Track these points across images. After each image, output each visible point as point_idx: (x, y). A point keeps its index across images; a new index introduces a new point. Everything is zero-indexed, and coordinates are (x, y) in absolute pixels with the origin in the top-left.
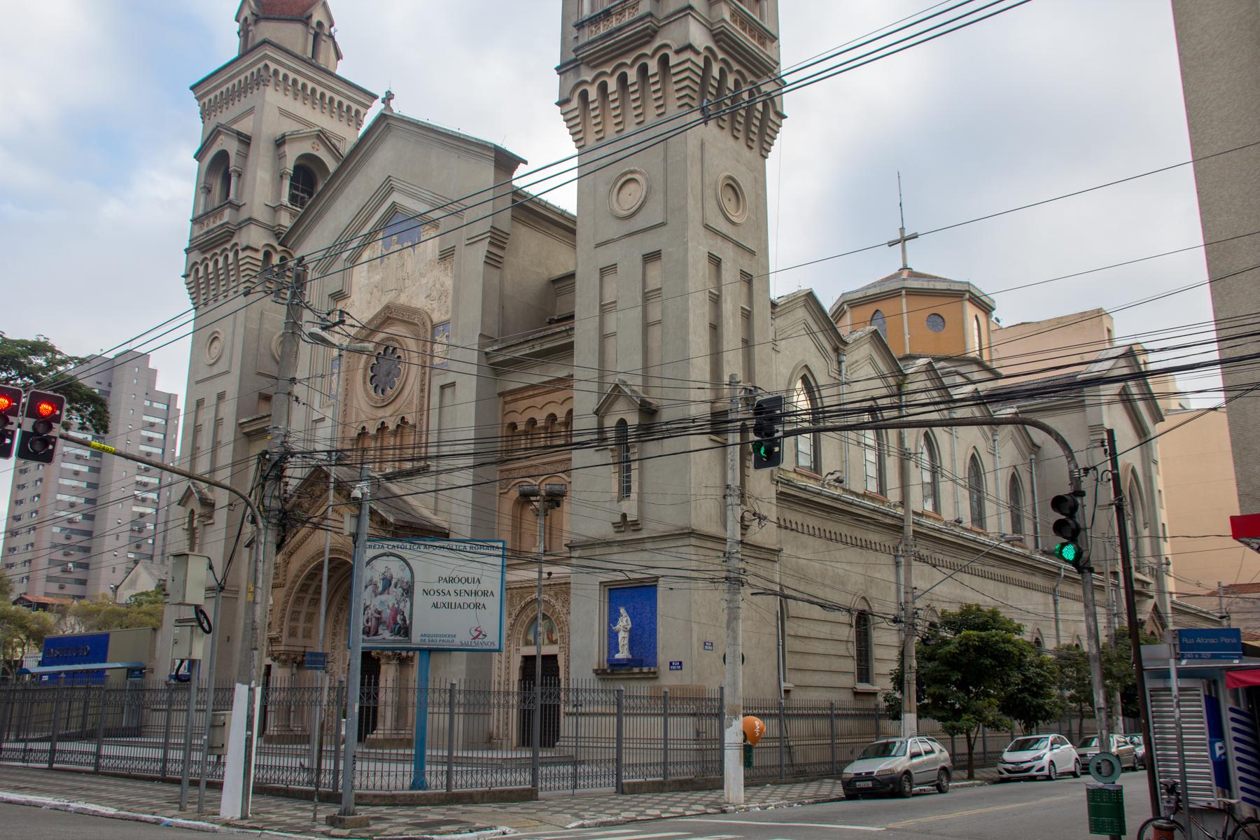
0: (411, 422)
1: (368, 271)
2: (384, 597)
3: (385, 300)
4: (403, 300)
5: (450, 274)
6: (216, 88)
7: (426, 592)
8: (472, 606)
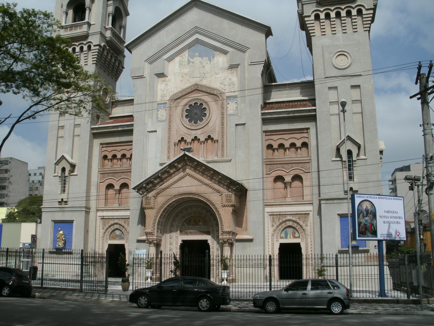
0: (215, 139)
1: (180, 67)
2: (367, 218)
3: (193, 81)
4: (205, 82)
5: (236, 76)
7: (381, 217)
8: (396, 223)
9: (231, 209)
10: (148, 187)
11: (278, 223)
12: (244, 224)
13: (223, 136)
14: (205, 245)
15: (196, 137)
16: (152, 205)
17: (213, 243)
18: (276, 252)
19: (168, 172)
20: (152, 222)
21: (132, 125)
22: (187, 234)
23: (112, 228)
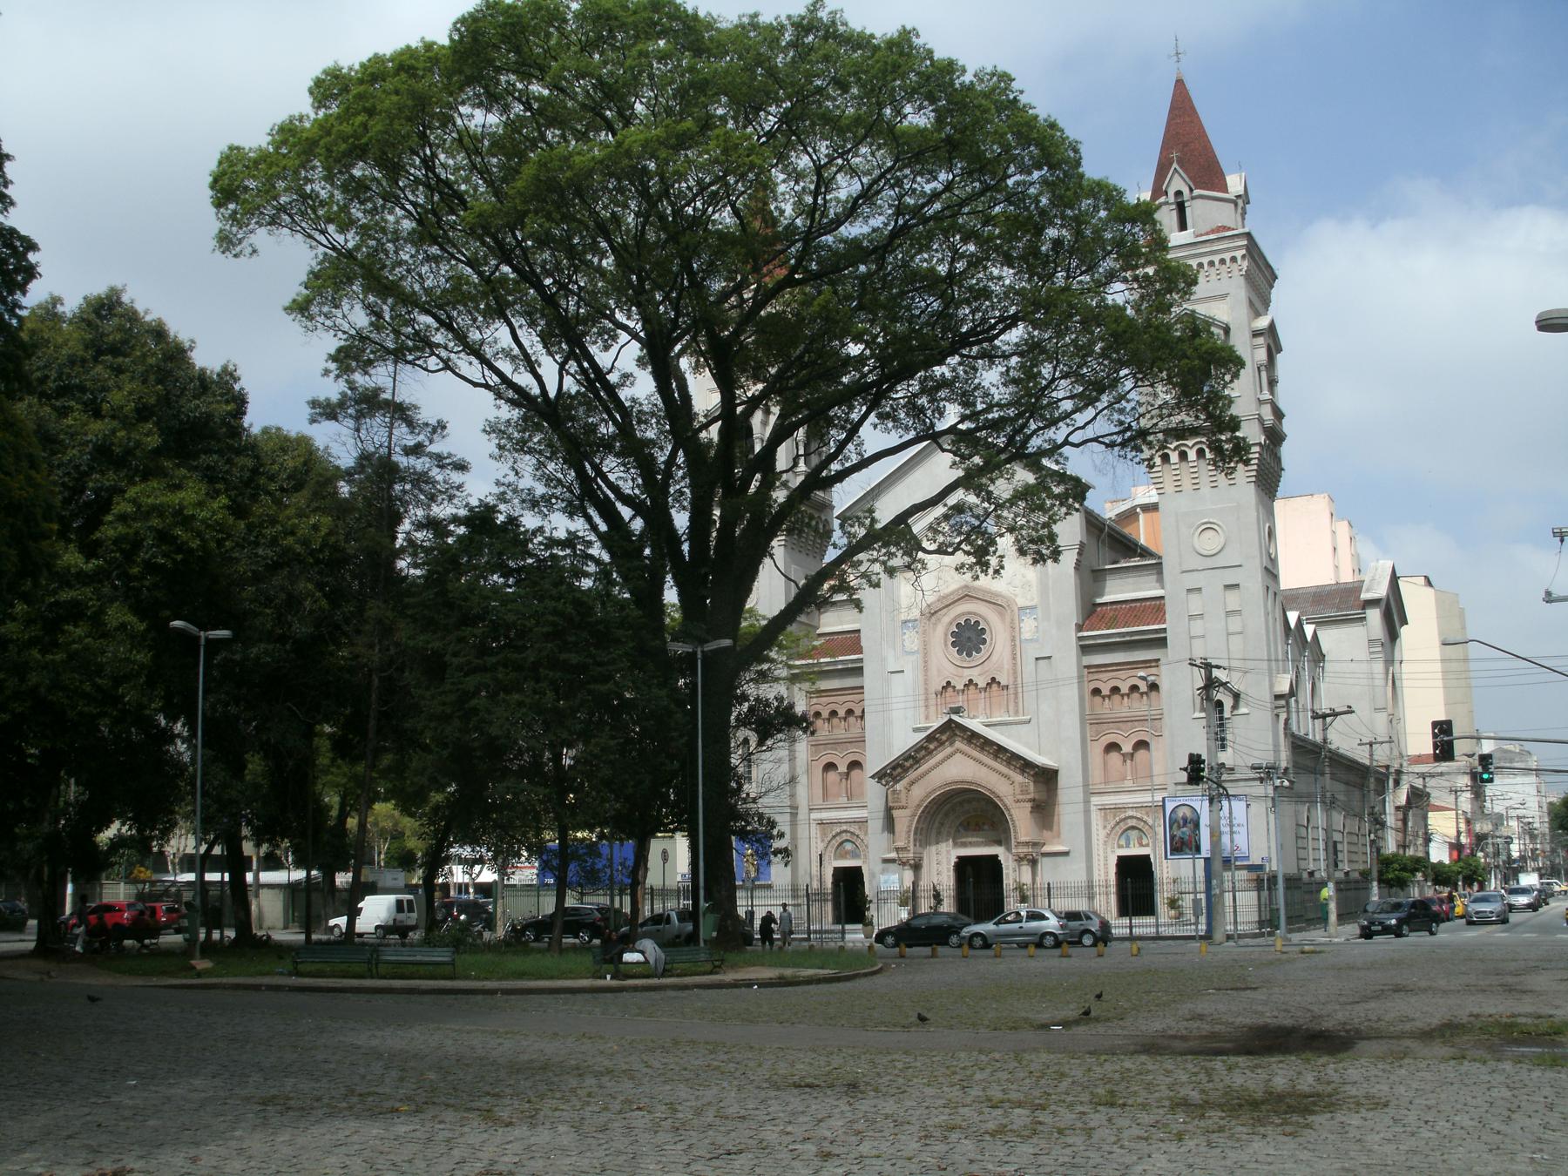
0: (1003, 683)
9: (1029, 805)
10: (895, 773)
11: (1113, 823)
12: (1055, 827)
13: (1016, 678)
14: (994, 862)
15: (971, 681)
16: (903, 803)
17: (1007, 860)
18: (1113, 870)
19: (926, 748)
20: (905, 829)
21: (861, 660)
22: (964, 845)
23: (839, 839)
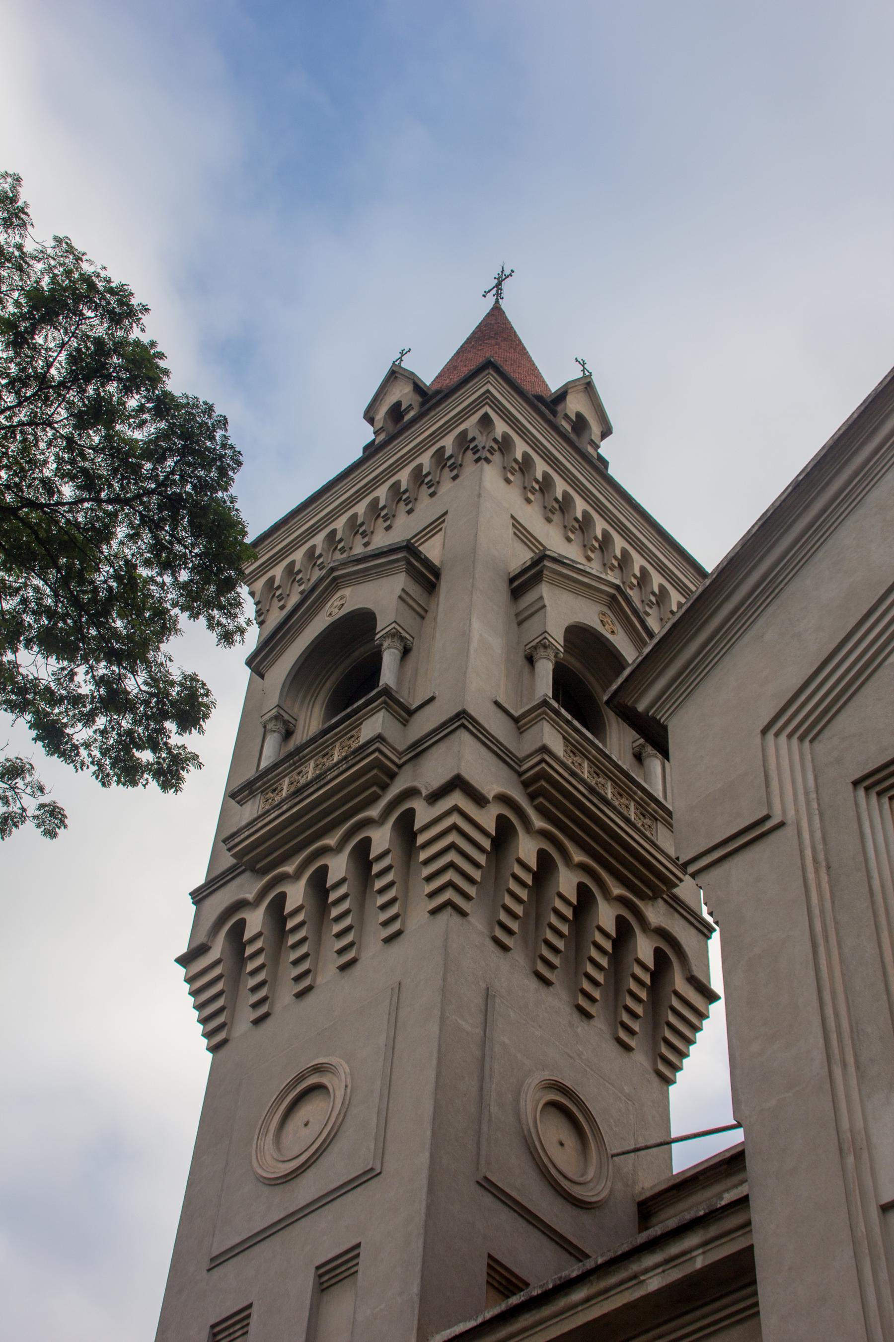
6: (312, 531)
